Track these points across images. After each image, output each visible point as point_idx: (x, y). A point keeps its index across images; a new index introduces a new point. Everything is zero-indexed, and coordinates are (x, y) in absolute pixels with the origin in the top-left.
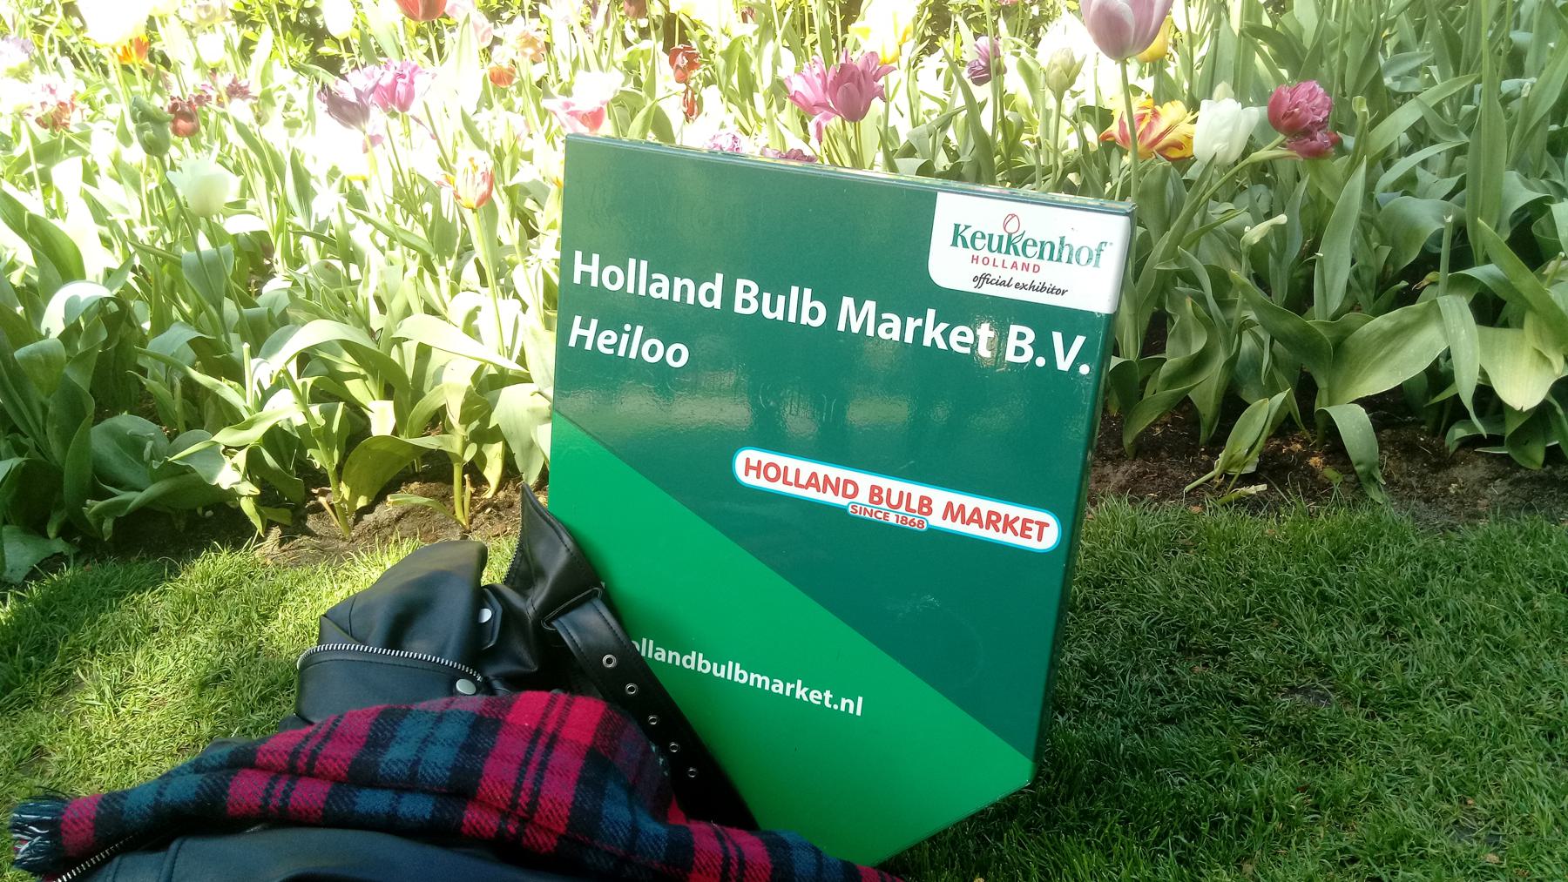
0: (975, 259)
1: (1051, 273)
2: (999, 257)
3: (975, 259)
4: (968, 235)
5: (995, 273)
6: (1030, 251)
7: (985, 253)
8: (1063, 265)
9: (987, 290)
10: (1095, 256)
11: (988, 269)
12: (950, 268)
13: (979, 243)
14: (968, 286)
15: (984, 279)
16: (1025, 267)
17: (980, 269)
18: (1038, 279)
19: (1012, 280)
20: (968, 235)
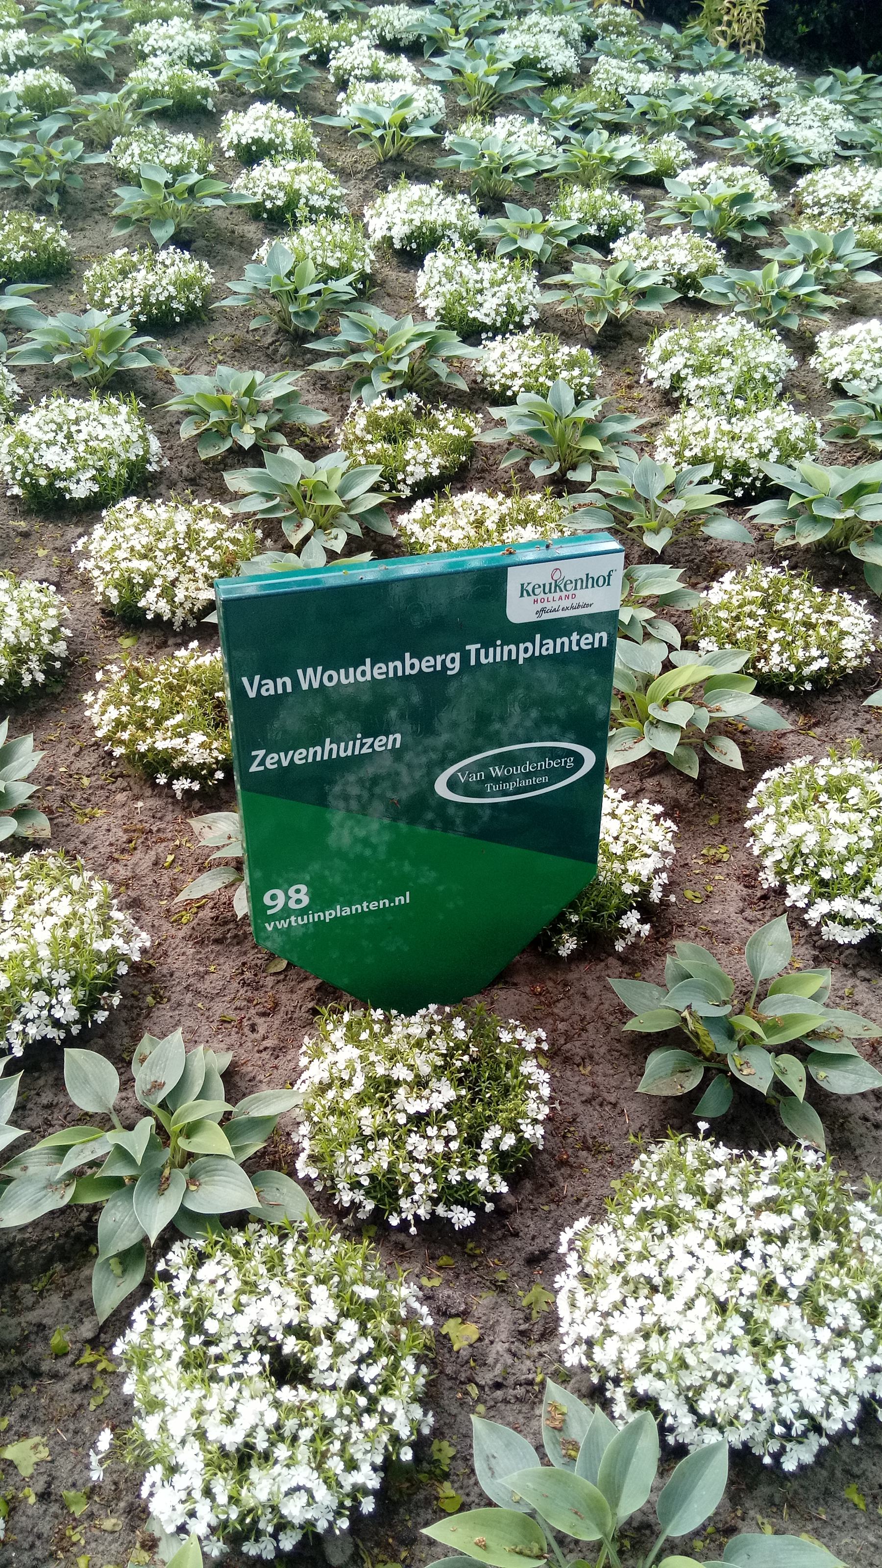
0: (535, 601)
1: (584, 595)
2: (550, 596)
3: (535, 601)
4: (530, 589)
5: (548, 606)
6: (569, 587)
7: (542, 595)
8: (590, 590)
9: (545, 617)
10: (607, 580)
11: (545, 604)
12: (520, 610)
13: (537, 591)
14: (534, 618)
15: (543, 610)
16: (567, 597)
17: (539, 606)
18: (575, 602)
19: (560, 607)
20: (530, 589)
